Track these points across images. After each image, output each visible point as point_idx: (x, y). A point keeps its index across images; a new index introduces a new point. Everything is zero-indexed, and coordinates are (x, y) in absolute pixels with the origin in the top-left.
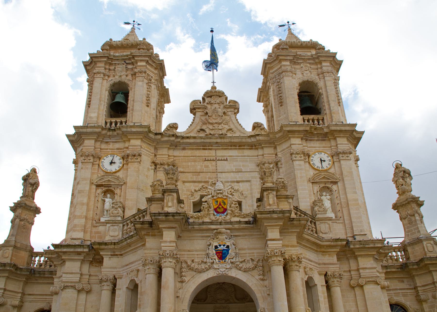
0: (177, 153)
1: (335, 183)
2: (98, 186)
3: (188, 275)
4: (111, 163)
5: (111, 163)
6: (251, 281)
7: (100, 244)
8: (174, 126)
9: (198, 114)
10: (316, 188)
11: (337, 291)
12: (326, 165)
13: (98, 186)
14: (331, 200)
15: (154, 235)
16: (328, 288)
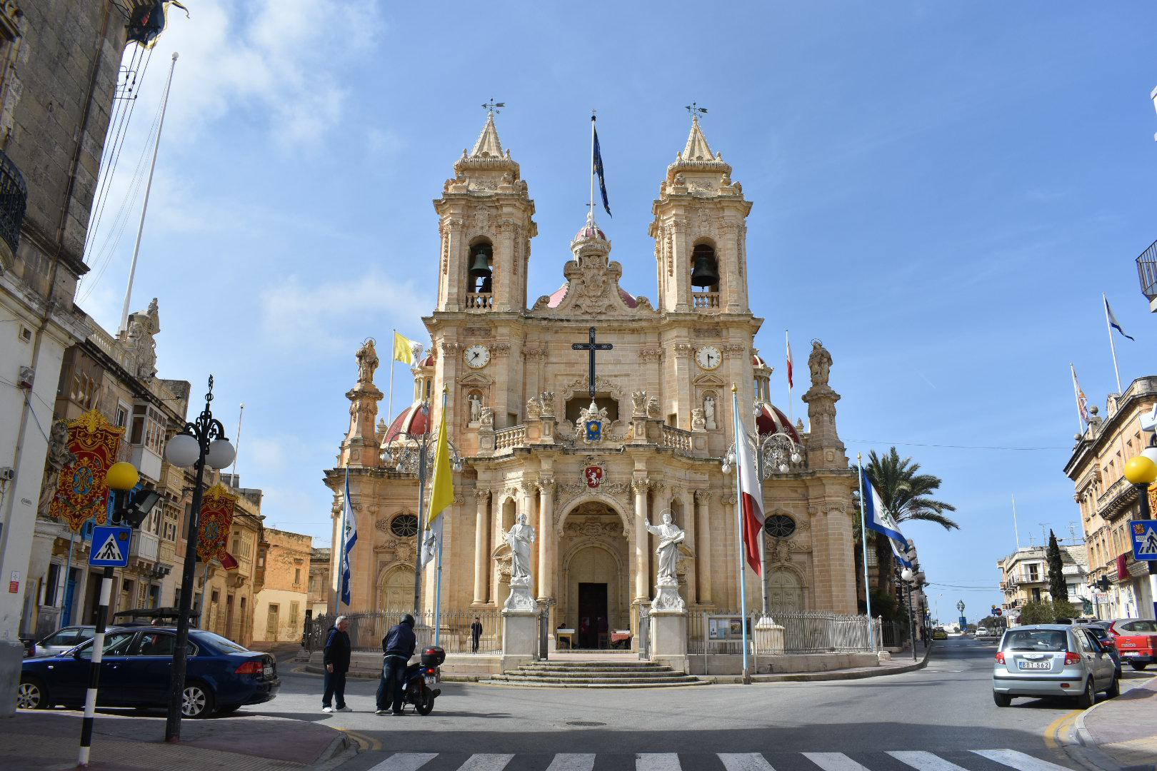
0: (548, 337)
1: (721, 387)
2: (463, 386)
3: (563, 497)
4: (477, 356)
5: (477, 356)
6: (618, 504)
7: (475, 460)
8: (544, 300)
9: (574, 282)
10: (700, 392)
11: (704, 511)
12: (714, 363)
13: (463, 386)
14: (715, 406)
15: (531, 459)
16: (697, 505)
